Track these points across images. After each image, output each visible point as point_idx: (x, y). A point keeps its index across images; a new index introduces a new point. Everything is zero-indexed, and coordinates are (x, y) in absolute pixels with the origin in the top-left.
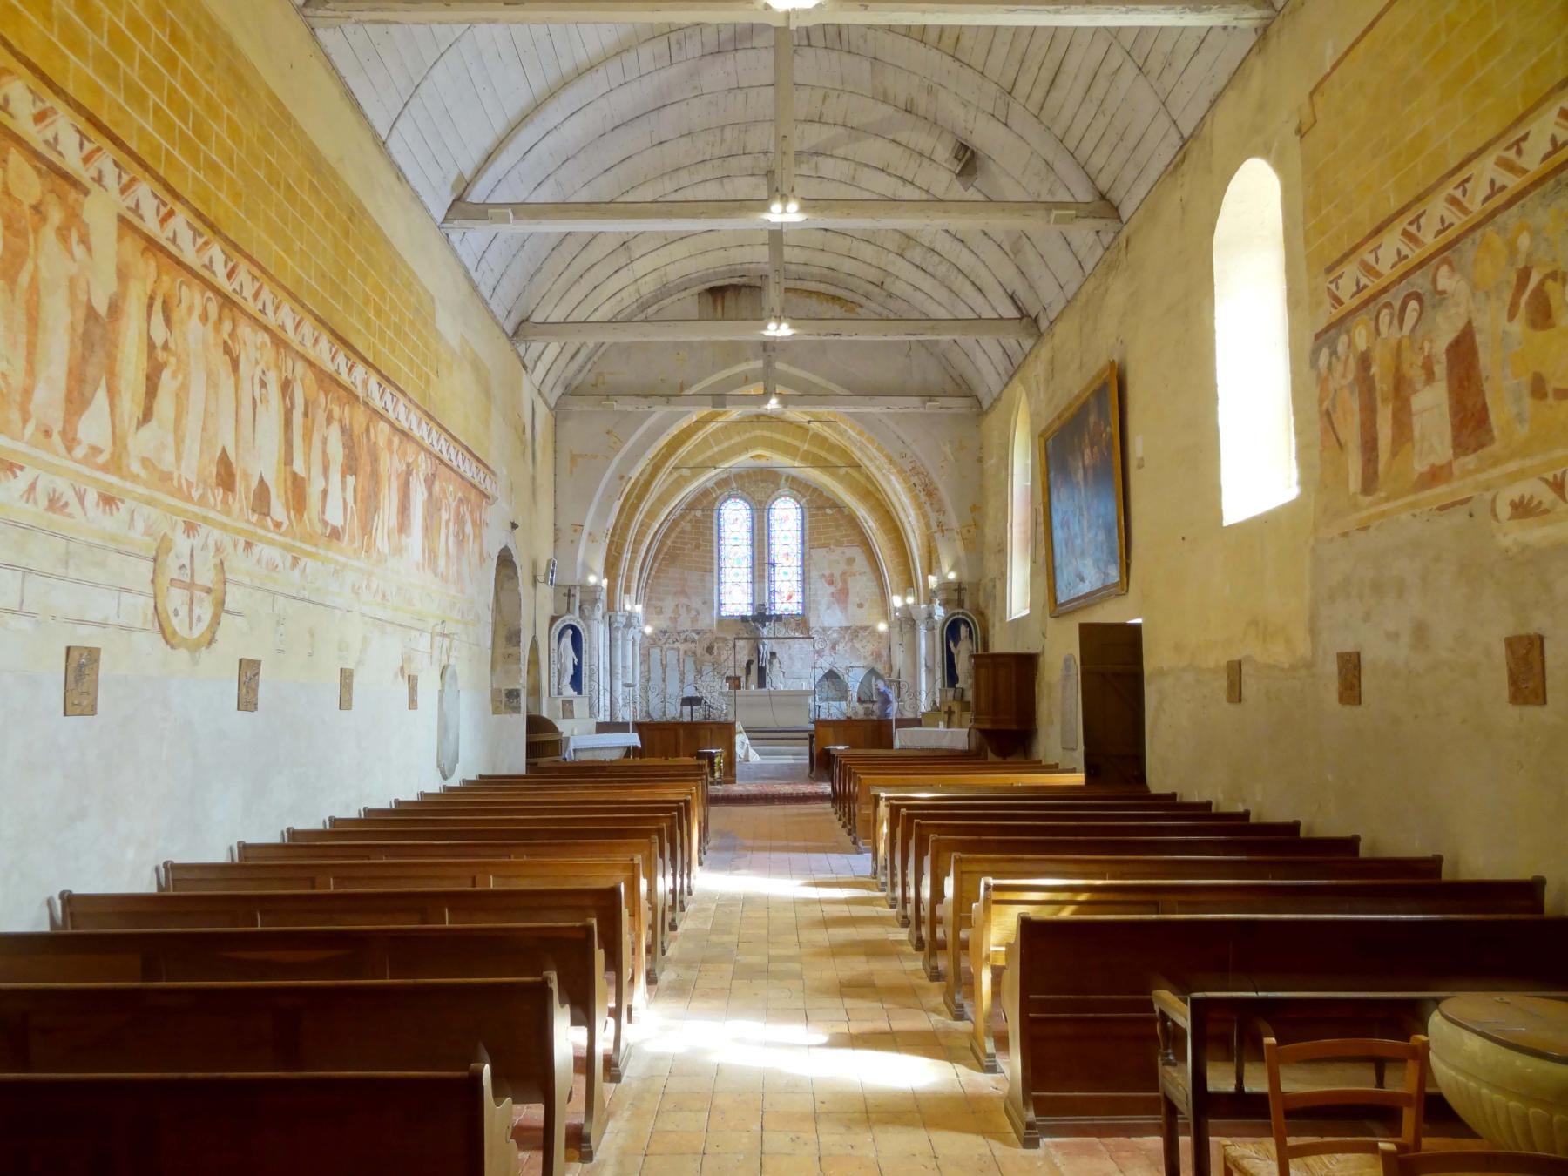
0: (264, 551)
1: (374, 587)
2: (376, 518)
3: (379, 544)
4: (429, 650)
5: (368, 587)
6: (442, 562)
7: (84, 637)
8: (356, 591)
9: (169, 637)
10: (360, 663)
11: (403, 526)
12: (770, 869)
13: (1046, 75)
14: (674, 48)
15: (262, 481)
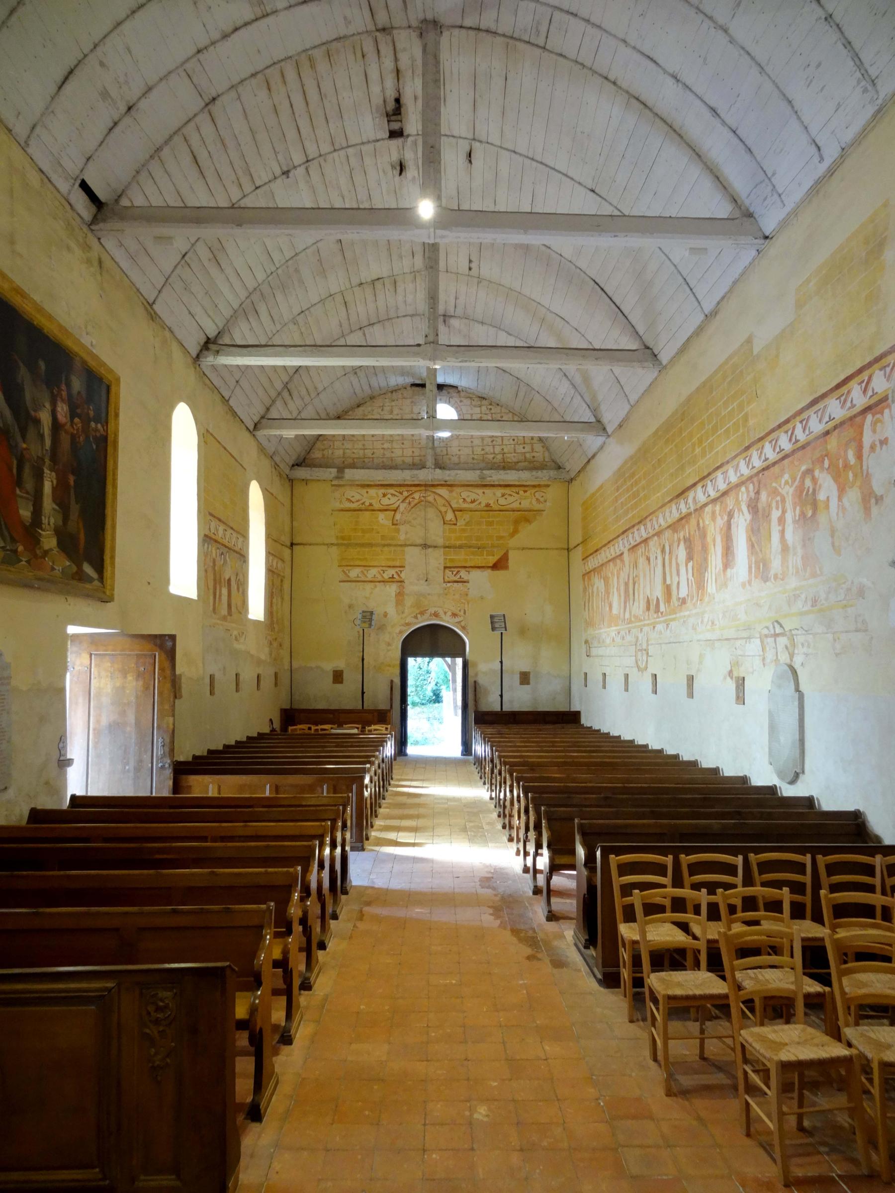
0: (660, 627)
1: (706, 620)
2: (706, 574)
3: (709, 590)
4: (762, 653)
5: (702, 622)
6: (776, 564)
7: (627, 671)
8: (694, 628)
9: (638, 667)
10: (699, 670)
11: (727, 564)
12: (452, 871)
13: (202, 156)
14: (543, 29)
15: (657, 598)
